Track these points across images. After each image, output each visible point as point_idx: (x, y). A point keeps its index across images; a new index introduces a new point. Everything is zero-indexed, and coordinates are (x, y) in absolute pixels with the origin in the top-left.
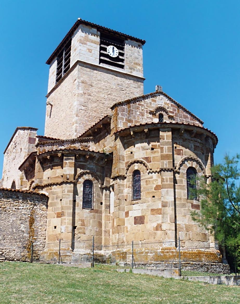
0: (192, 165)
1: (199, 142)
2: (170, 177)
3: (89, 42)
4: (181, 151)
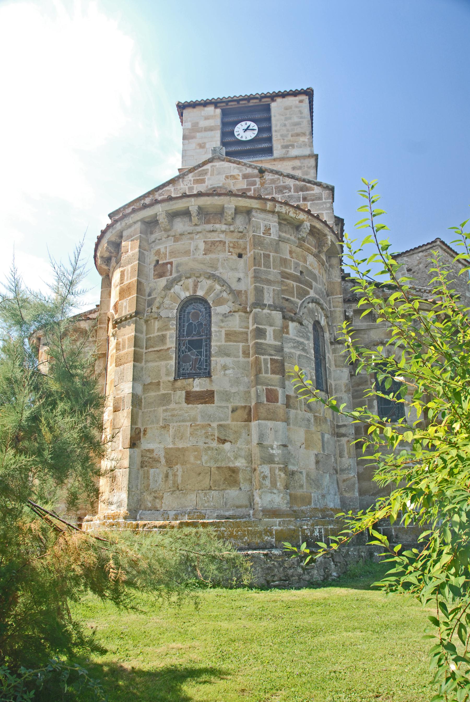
0: (195, 291)
1: (223, 232)
2: (130, 335)
3: (199, 132)
4: (169, 266)
